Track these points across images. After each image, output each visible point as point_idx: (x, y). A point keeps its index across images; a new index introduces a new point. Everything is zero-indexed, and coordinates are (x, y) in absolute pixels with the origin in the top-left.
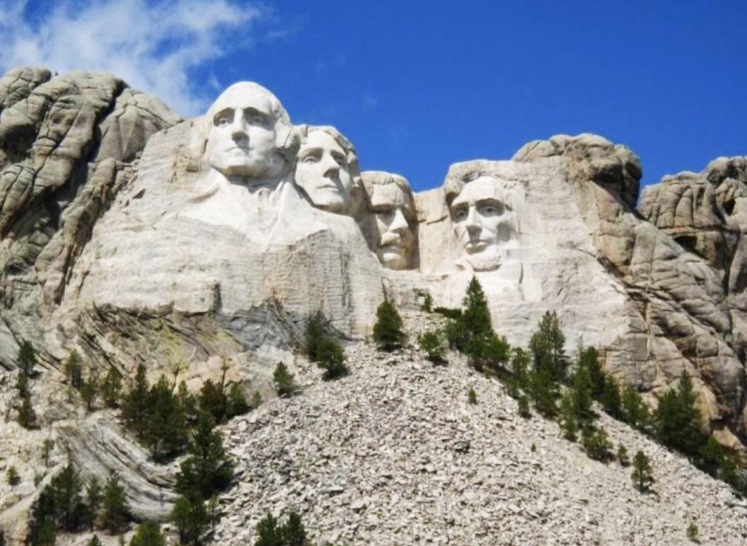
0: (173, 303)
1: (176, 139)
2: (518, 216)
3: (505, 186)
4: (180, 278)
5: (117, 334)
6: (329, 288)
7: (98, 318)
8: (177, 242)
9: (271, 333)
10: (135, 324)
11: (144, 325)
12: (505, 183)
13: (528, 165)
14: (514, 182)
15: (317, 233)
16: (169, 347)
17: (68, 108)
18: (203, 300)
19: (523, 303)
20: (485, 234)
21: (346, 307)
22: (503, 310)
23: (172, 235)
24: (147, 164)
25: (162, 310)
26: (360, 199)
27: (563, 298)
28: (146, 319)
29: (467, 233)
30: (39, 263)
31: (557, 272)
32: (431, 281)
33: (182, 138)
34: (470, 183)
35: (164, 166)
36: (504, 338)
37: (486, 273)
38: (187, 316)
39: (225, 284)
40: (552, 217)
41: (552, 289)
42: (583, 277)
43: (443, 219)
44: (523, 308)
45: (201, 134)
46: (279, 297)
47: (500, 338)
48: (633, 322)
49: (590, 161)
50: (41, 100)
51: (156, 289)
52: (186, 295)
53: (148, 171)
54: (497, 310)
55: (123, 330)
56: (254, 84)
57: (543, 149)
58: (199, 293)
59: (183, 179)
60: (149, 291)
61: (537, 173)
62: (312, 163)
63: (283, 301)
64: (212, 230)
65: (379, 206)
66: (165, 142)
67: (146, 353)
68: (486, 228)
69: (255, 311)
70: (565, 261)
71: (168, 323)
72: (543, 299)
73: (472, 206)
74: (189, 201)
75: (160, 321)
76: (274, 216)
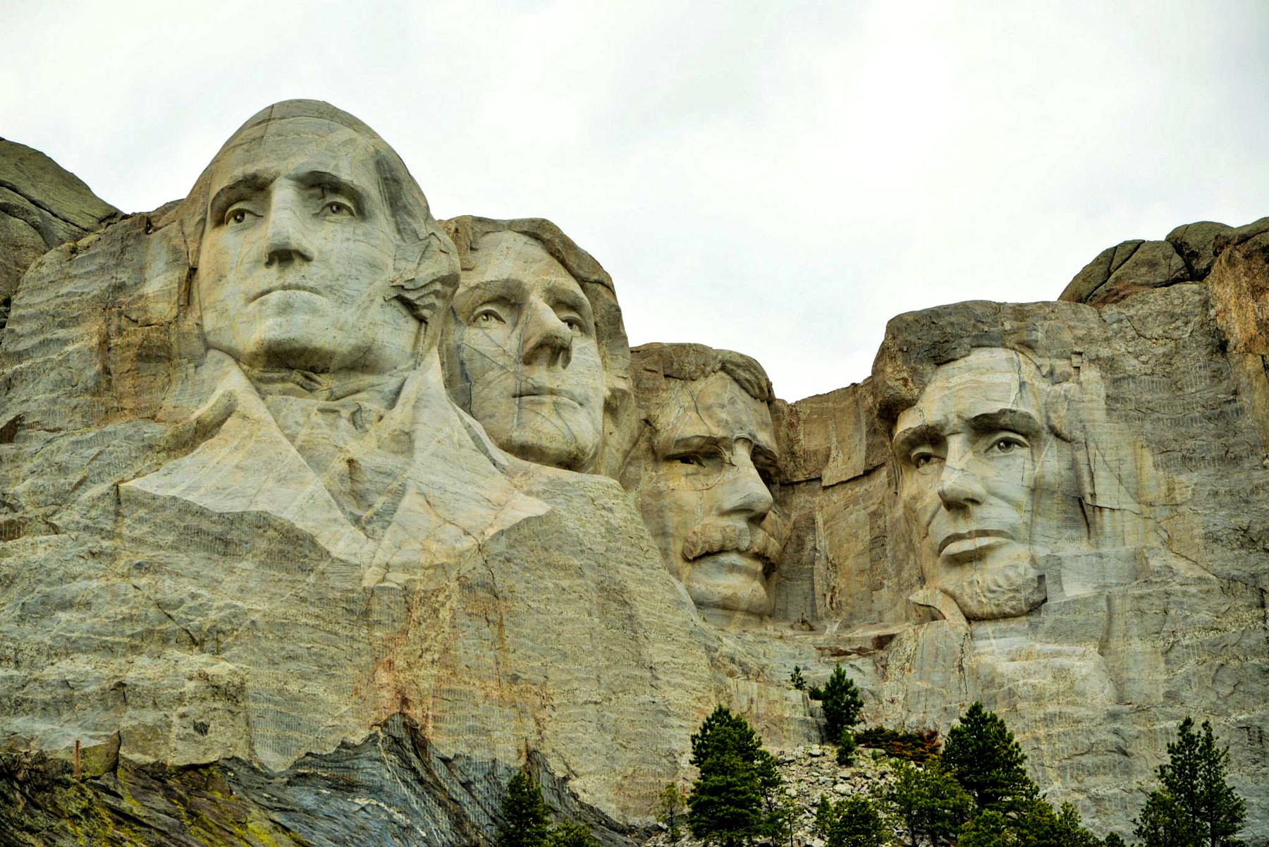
1: (102, 268)
3: (1051, 373)
4: (142, 669)
6: (559, 684)
8: (122, 565)
9: (398, 817)
10: (11, 803)
11: (37, 807)
12: (1046, 363)
13: (1110, 311)
14: (1076, 360)
15: (517, 527)
19: (1112, 707)
20: (995, 514)
21: (609, 738)
23: (105, 543)
24: (22, 346)
26: (631, 418)
27: (1228, 691)
28: (41, 788)
29: (943, 508)
31: (1205, 616)
32: (840, 653)
33: (117, 265)
34: (946, 367)
35: (70, 348)
36: (1066, 806)
37: (1002, 625)
38: (156, 776)
39: (261, 679)
40: (1187, 461)
43: (868, 473)
44: (1117, 725)
45: (175, 250)
46: (416, 713)
47: (1057, 812)
51: (69, 702)
52: (150, 717)
53: (25, 364)
54: (1042, 732)
57: (1152, 265)
58: (194, 709)
59: (129, 382)
60: (45, 706)
61: (1140, 336)
62: (493, 322)
63: (430, 726)
64: (218, 529)
65: (684, 442)
66: (71, 277)
68: (994, 494)
69: (350, 758)
70: (1229, 584)
71: (109, 800)
72: (1170, 696)
73: (955, 433)
74: (151, 447)
75: (83, 795)
76: (395, 485)
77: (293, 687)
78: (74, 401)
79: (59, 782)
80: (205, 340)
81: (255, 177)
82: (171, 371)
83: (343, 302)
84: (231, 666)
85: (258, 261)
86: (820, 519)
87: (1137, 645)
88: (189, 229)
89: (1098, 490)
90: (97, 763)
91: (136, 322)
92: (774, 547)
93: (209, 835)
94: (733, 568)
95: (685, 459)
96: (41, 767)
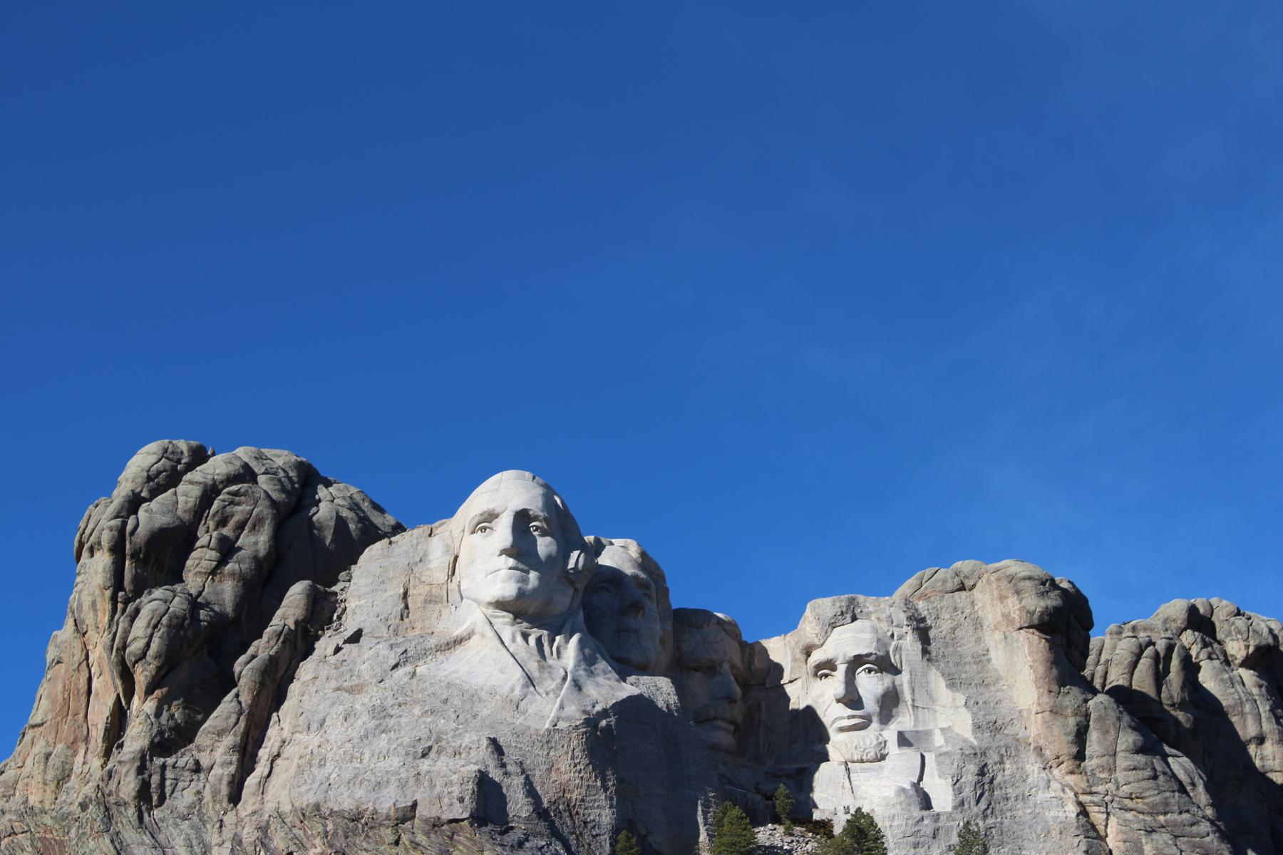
0: (414, 806)
2: (911, 682)
3: (892, 636)
14: (905, 629)
17: (239, 504)
18: (461, 800)
22: (896, 823)
25: (400, 814)
30: (202, 738)
31: (972, 768)
38: (436, 824)
41: (968, 792)
42: (1013, 776)
45: (447, 546)
48: (1090, 846)
49: (1021, 601)
50: (196, 492)
56: (528, 475)
57: (945, 581)
72: (955, 808)
76: (563, 673)
78: (390, 622)
84: (476, 768)
86: (763, 705)
87: (938, 781)
89: (917, 697)
92: (739, 718)
94: (719, 728)
95: (696, 670)
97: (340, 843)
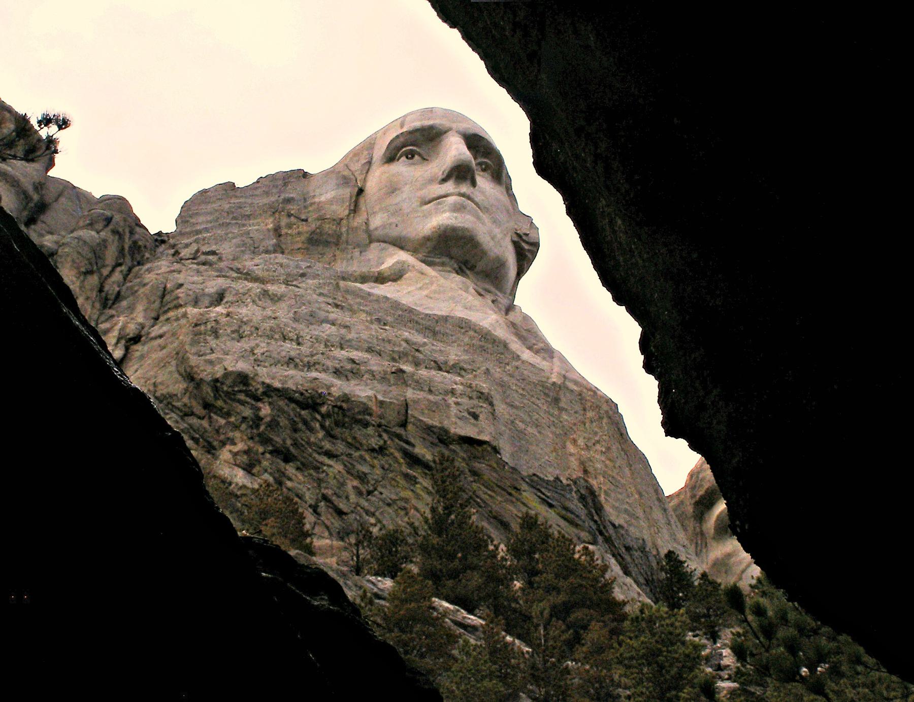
5: (261, 450)
7: (199, 410)
10: (311, 430)
16: (407, 494)
18: (475, 416)
28: (337, 424)
38: (442, 438)
45: (344, 177)
46: (594, 482)
55: (278, 440)
67: (347, 498)
75: (380, 436)
77: (521, 425)
79: (358, 421)
80: (370, 236)
81: (431, 127)
82: (338, 253)
83: (495, 221)
85: (431, 181)
88: (356, 167)
90: (392, 416)
91: (306, 220)
93: (489, 492)
96: (345, 405)
97: (282, 438)
